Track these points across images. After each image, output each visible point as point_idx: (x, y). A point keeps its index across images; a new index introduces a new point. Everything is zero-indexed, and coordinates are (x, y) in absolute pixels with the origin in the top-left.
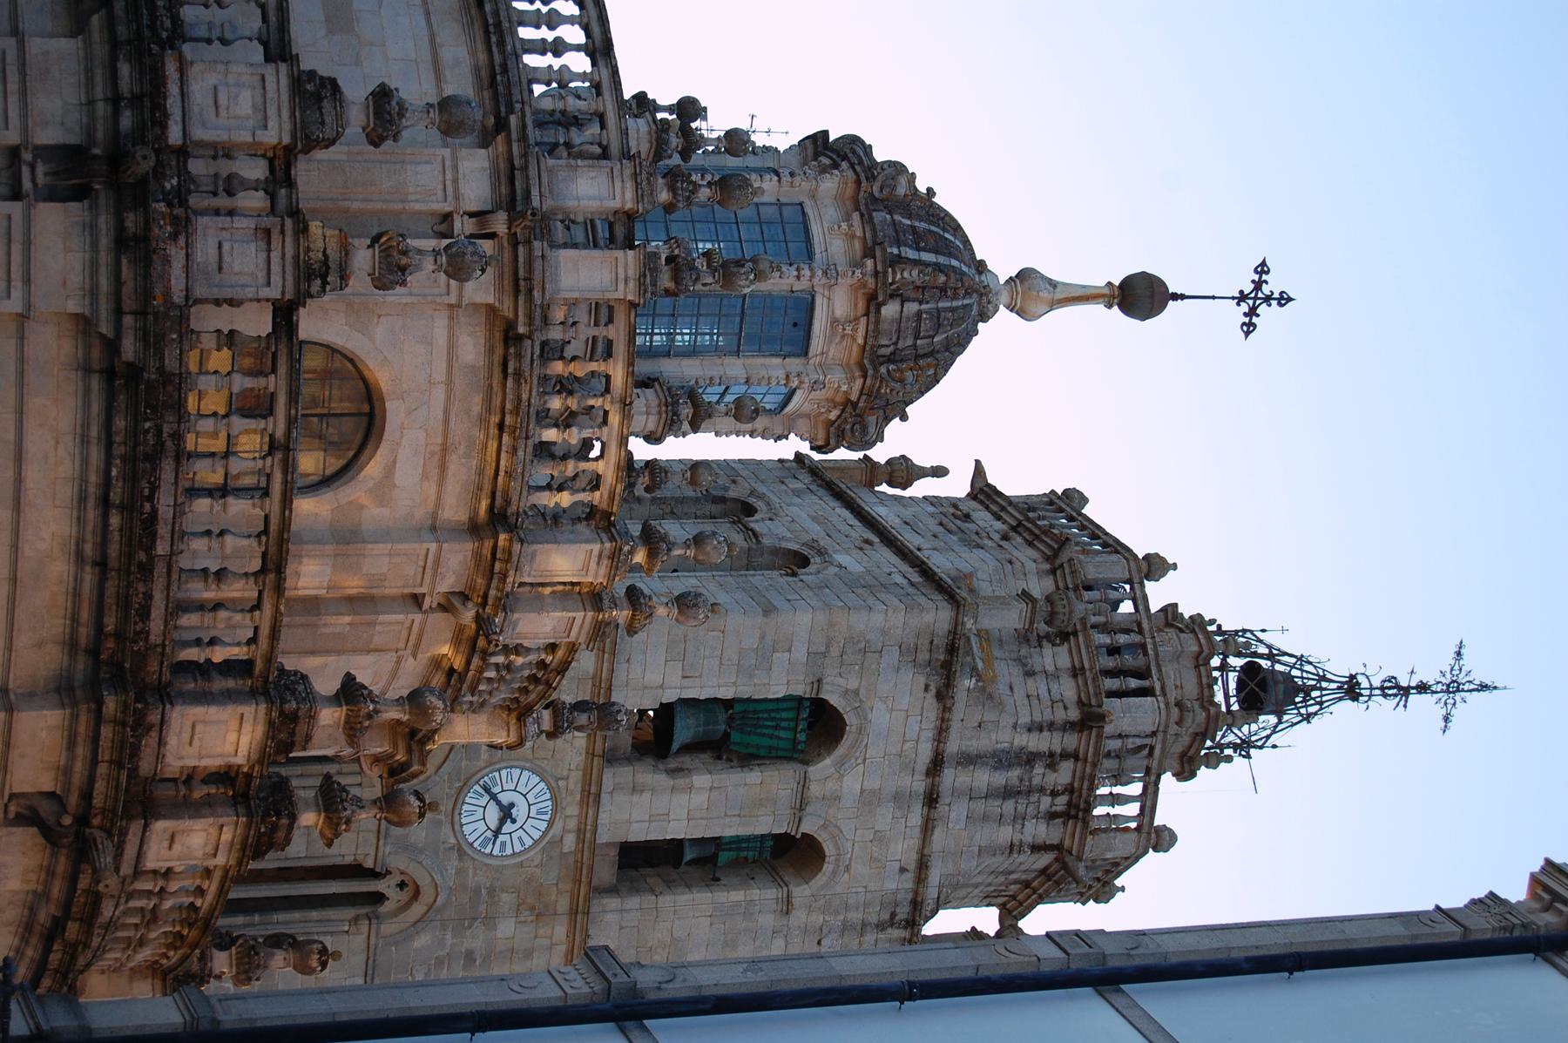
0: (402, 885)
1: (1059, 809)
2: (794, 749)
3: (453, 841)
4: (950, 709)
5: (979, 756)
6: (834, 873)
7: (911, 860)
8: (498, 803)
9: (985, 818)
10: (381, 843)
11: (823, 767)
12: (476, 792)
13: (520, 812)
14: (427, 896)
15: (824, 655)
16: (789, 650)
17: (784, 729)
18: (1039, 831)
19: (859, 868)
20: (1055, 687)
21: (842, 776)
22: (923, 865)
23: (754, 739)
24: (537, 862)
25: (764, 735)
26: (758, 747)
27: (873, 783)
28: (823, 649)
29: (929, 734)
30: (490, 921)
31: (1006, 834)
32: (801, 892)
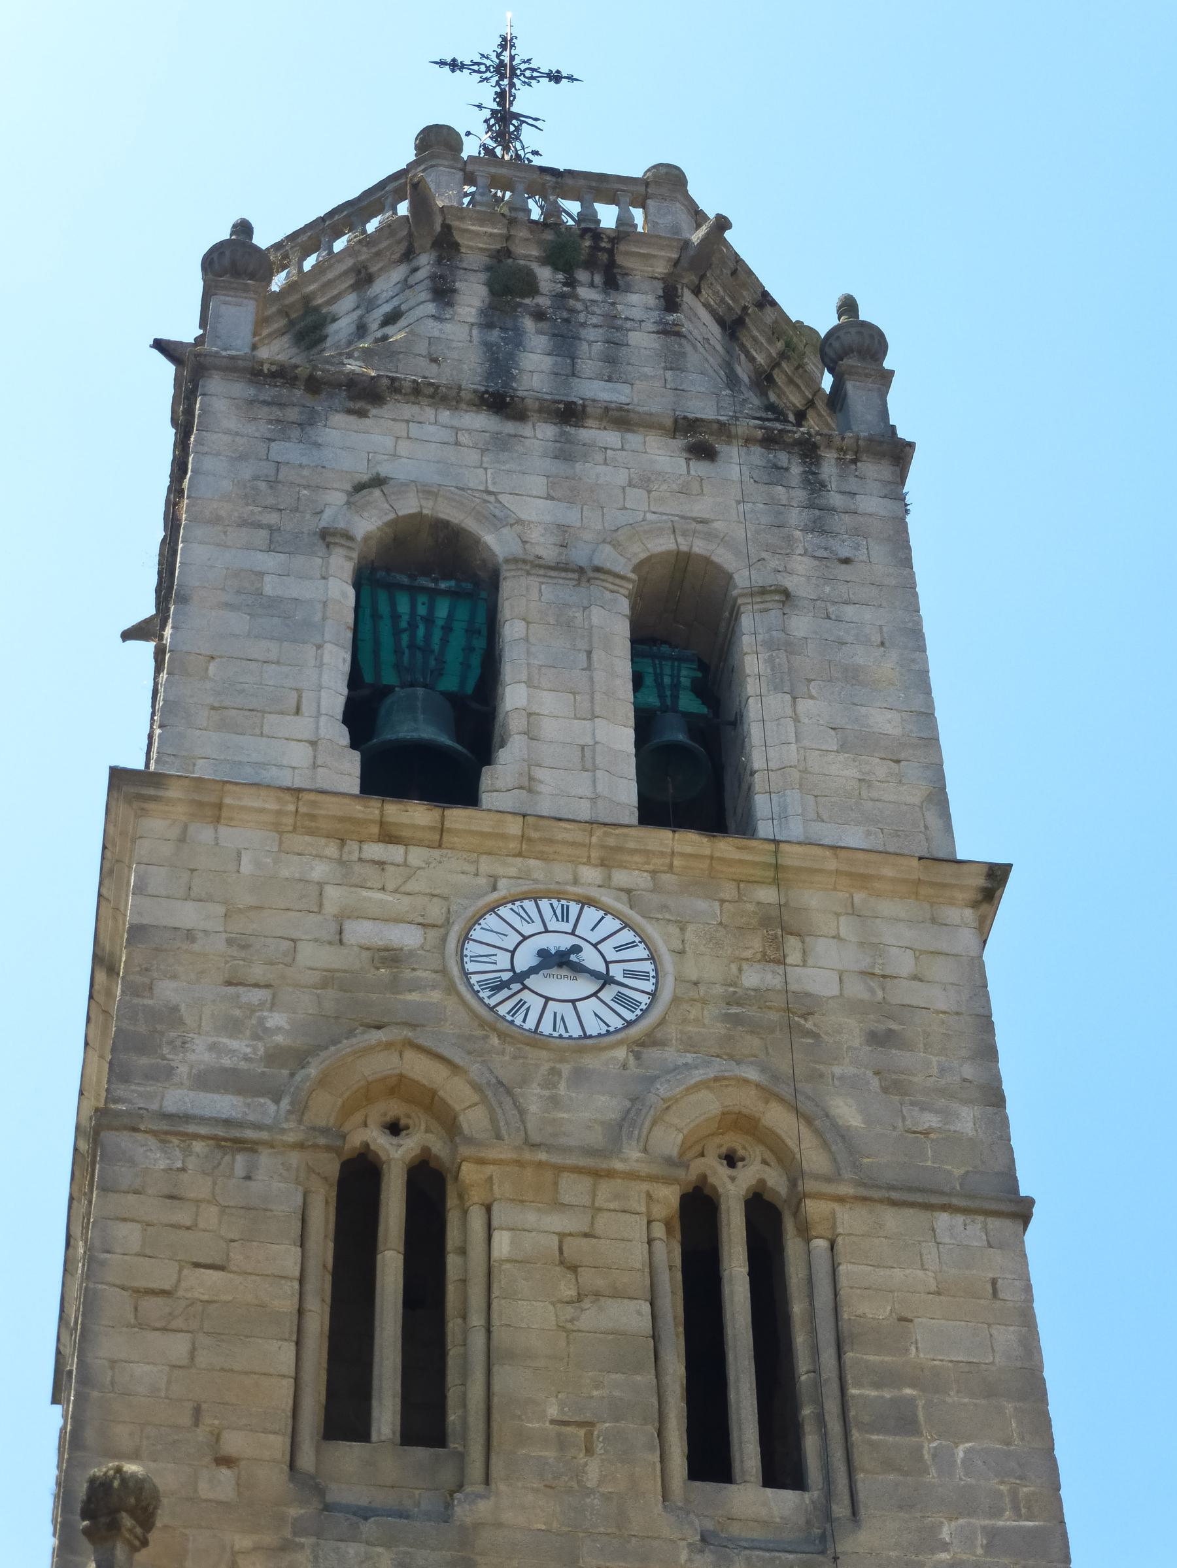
0: (731, 1160)
1: (598, 279)
6: (710, 536)
8: (533, 970)
9: (611, 361)
10: (618, 1165)
12: (514, 1011)
13: (557, 942)
14: (747, 1101)
16: (261, 574)
17: (431, 608)
21: (519, 521)
23: (454, 654)
24: (673, 930)
25: (445, 641)
26: (469, 649)
27: (538, 484)
28: (264, 533)
29: (445, 415)
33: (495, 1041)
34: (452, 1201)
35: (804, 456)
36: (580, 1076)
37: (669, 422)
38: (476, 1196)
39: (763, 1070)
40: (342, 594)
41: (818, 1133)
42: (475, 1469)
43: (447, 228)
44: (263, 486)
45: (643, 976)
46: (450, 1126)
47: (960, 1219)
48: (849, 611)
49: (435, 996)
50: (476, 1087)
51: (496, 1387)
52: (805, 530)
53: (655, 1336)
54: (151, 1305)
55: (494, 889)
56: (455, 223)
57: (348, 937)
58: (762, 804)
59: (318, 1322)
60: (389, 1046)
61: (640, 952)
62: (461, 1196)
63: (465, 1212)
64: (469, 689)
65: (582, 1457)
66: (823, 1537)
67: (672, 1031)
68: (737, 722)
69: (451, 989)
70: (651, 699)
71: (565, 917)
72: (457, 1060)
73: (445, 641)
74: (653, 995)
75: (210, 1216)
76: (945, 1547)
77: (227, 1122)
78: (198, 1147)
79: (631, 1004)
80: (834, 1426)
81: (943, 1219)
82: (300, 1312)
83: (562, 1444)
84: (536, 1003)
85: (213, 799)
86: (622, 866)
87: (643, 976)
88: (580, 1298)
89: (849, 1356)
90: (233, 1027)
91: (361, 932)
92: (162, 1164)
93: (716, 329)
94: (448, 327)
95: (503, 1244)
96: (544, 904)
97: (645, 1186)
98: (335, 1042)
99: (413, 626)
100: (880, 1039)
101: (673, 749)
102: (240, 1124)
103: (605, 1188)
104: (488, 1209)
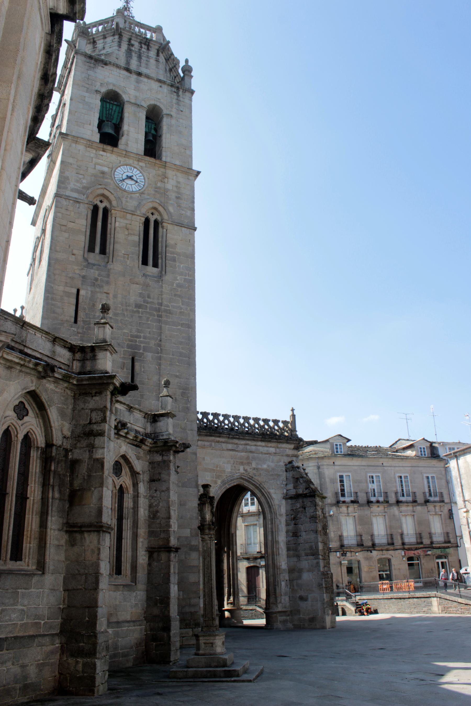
0: (152, 214)
1: (146, 47)
2: (119, 106)
3: (138, 195)
4: (110, 62)
5: (127, 61)
6: (160, 102)
7: (158, 84)
8: (126, 179)
9: (147, 64)
10: (136, 214)
11: (125, 97)
12: (122, 185)
13: (130, 174)
14: (156, 205)
15: (88, 88)
16: (85, 97)
17: (112, 107)
18: (153, 53)
19: (159, 96)
20: (108, 42)
21: (129, 94)
22: (159, 81)
23: (115, 116)
24: (148, 174)
25: (114, 114)
26: (118, 116)
28: (86, 89)
29: (118, 70)
30: (166, 190)
31: (152, 61)
32: (165, 111)
33: (118, 190)
34: (109, 215)
35: (177, 90)
36: (131, 198)
37: (156, 79)
38: (114, 216)
39: (159, 201)
40: (99, 103)
41: (166, 212)
42: (111, 260)
43: (121, 32)
44: (86, 79)
45: (142, 182)
46: (110, 202)
47: (186, 229)
48: (181, 121)
49: (109, 181)
50: (115, 197)
51: (115, 247)
52: (176, 104)
53: (139, 242)
54: (62, 227)
55: (120, 163)
56: (123, 31)
57: (96, 168)
58: (164, 154)
59: (88, 233)
60: (102, 188)
61: (142, 178)
62: (111, 215)
63: (112, 218)
64: (117, 123)
65: (127, 260)
66: (161, 276)
67: (146, 192)
68: (160, 136)
69: (112, 180)
70: (147, 130)
71: (131, 170)
72: (112, 192)
73: (114, 114)
74: (144, 185)
75: (72, 214)
76: (178, 280)
77: (76, 198)
78: (71, 201)
79: (140, 186)
80: (164, 259)
81: (183, 229)
82: (86, 231)
83: (124, 258)
84: (125, 184)
85: (76, 140)
86: (141, 162)
87: (142, 182)
88: (128, 234)
89: (167, 249)
90: (77, 181)
91: (98, 167)
92: (65, 204)
93: (164, 60)
94: (119, 52)
95: (117, 224)
96: (128, 167)
97: (140, 217)
98: (93, 187)
99: (109, 110)
100: (178, 198)
101: (150, 140)
102: (78, 199)
103: (134, 217)
104: (115, 218)
